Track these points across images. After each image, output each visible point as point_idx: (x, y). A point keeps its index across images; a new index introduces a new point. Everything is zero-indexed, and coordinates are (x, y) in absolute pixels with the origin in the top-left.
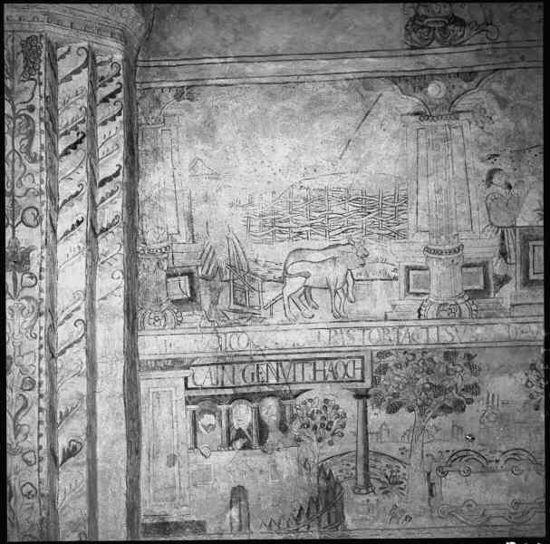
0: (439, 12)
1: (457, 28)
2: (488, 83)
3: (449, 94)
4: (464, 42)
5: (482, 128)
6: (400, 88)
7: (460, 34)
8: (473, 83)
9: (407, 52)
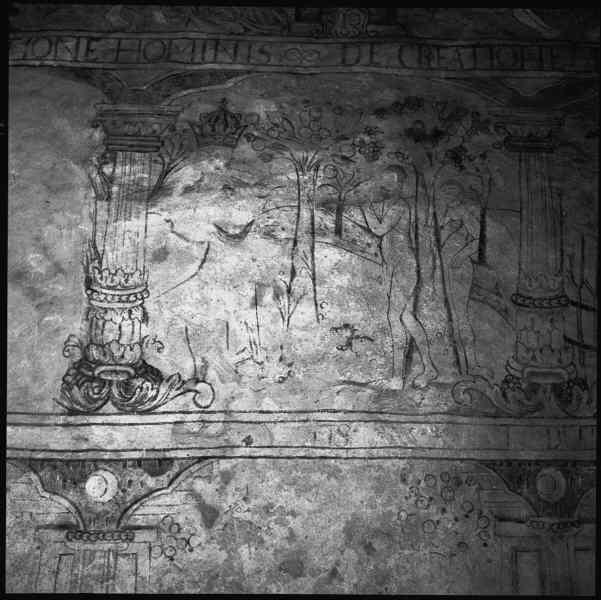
0: (123, 357)
1: (149, 384)
2: (190, 480)
3: (121, 494)
4: (156, 407)
5: (172, 559)
6: (40, 478)
7: (151, 393)
8: (161, 478)
9: (61, 420)
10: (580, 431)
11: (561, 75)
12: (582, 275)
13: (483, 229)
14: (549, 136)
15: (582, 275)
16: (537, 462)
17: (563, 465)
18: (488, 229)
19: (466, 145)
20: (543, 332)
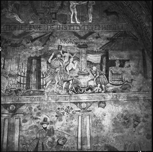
10: (19, 98)
11: (23, 31)
12: (22, 70)
13: (4, 62)
14: (19, 43)
15: (22, 70)
16: (10, 104)
17: (14, 104)
18: (5, 62)
19: (3, 46)
20: (14, 81)
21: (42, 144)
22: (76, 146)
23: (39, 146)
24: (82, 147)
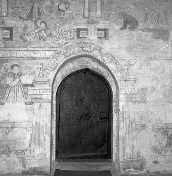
21: (39, 9)
22: (82, 13)
23: (33, 11)
24: (90, 14)
